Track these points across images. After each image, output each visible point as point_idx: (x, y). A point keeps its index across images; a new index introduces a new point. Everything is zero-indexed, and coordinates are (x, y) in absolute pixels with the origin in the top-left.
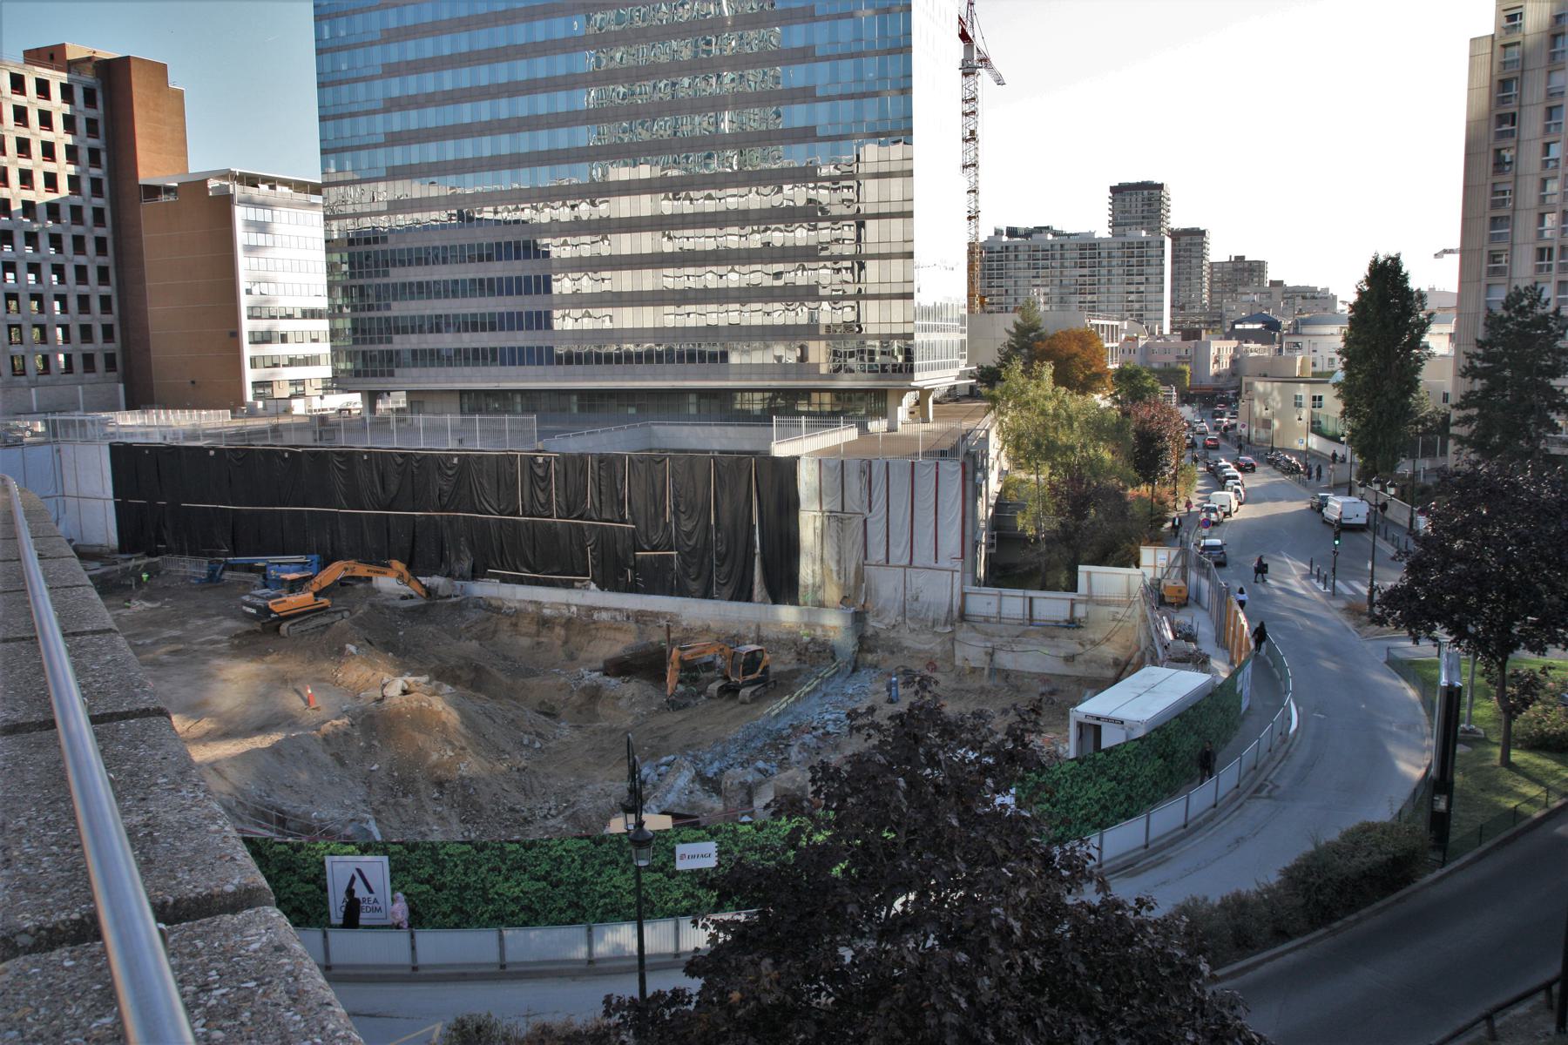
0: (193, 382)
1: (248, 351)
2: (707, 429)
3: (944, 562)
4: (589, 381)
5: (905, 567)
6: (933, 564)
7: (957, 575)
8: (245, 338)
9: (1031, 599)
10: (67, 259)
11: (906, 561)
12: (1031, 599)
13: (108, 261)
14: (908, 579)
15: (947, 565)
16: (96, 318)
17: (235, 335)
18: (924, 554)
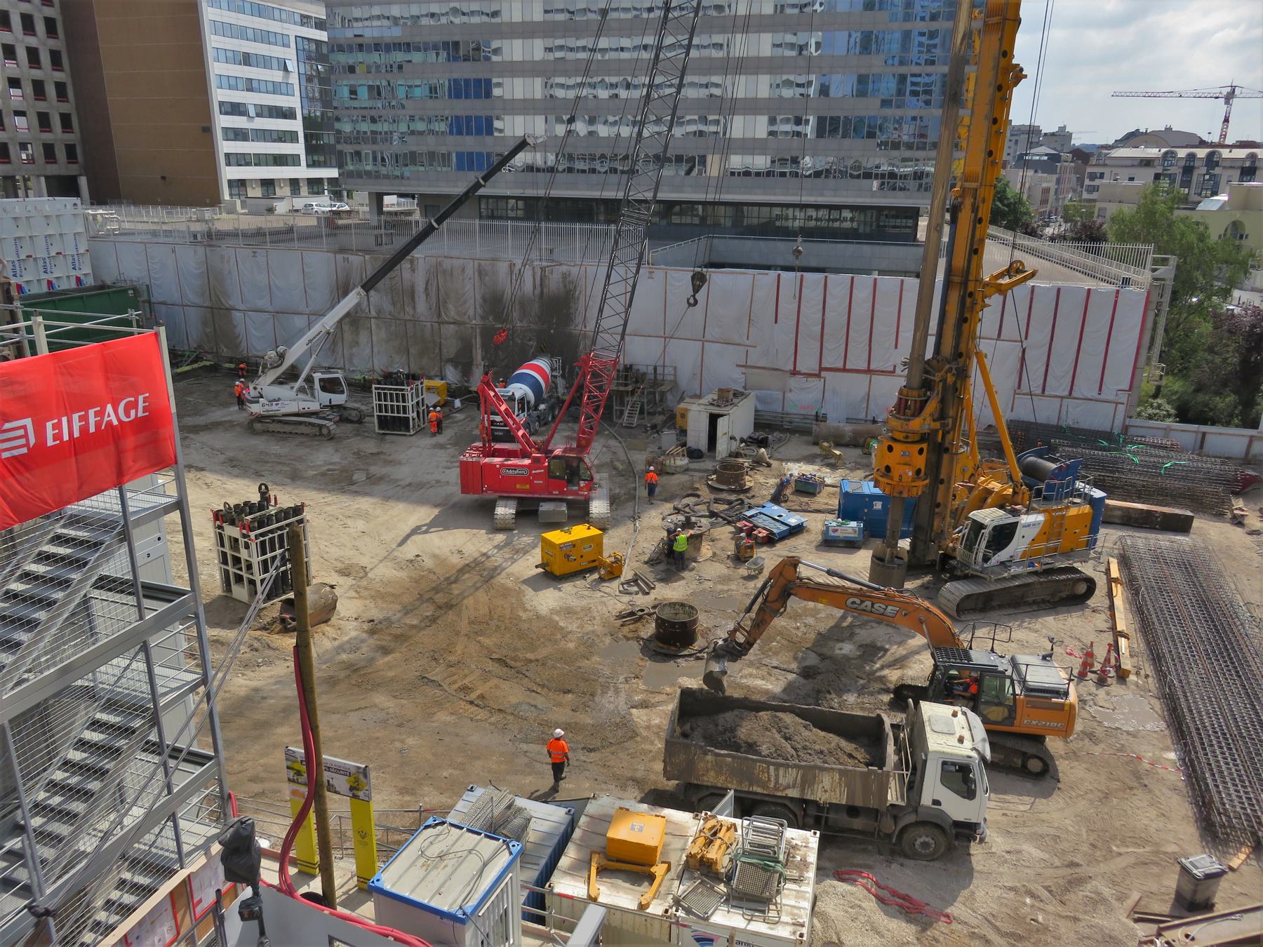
0: (163, 178)
1: (226, 147)
2: (771, 244)
3: (1108, 394)
4: (744, 193)
5: (1062, 398)
6: (1094, 394)
7: (1121, 408)
8: (219, 134)
9: (1204, 434)
10: (17, 39)
11: (1066, 393)
12: (1204, 434)
13: (59, 44)
14: (1064, 408)
15: (1111, 397)
16: (53, 106)
17: (208, 130)
18: (1085, 387)
